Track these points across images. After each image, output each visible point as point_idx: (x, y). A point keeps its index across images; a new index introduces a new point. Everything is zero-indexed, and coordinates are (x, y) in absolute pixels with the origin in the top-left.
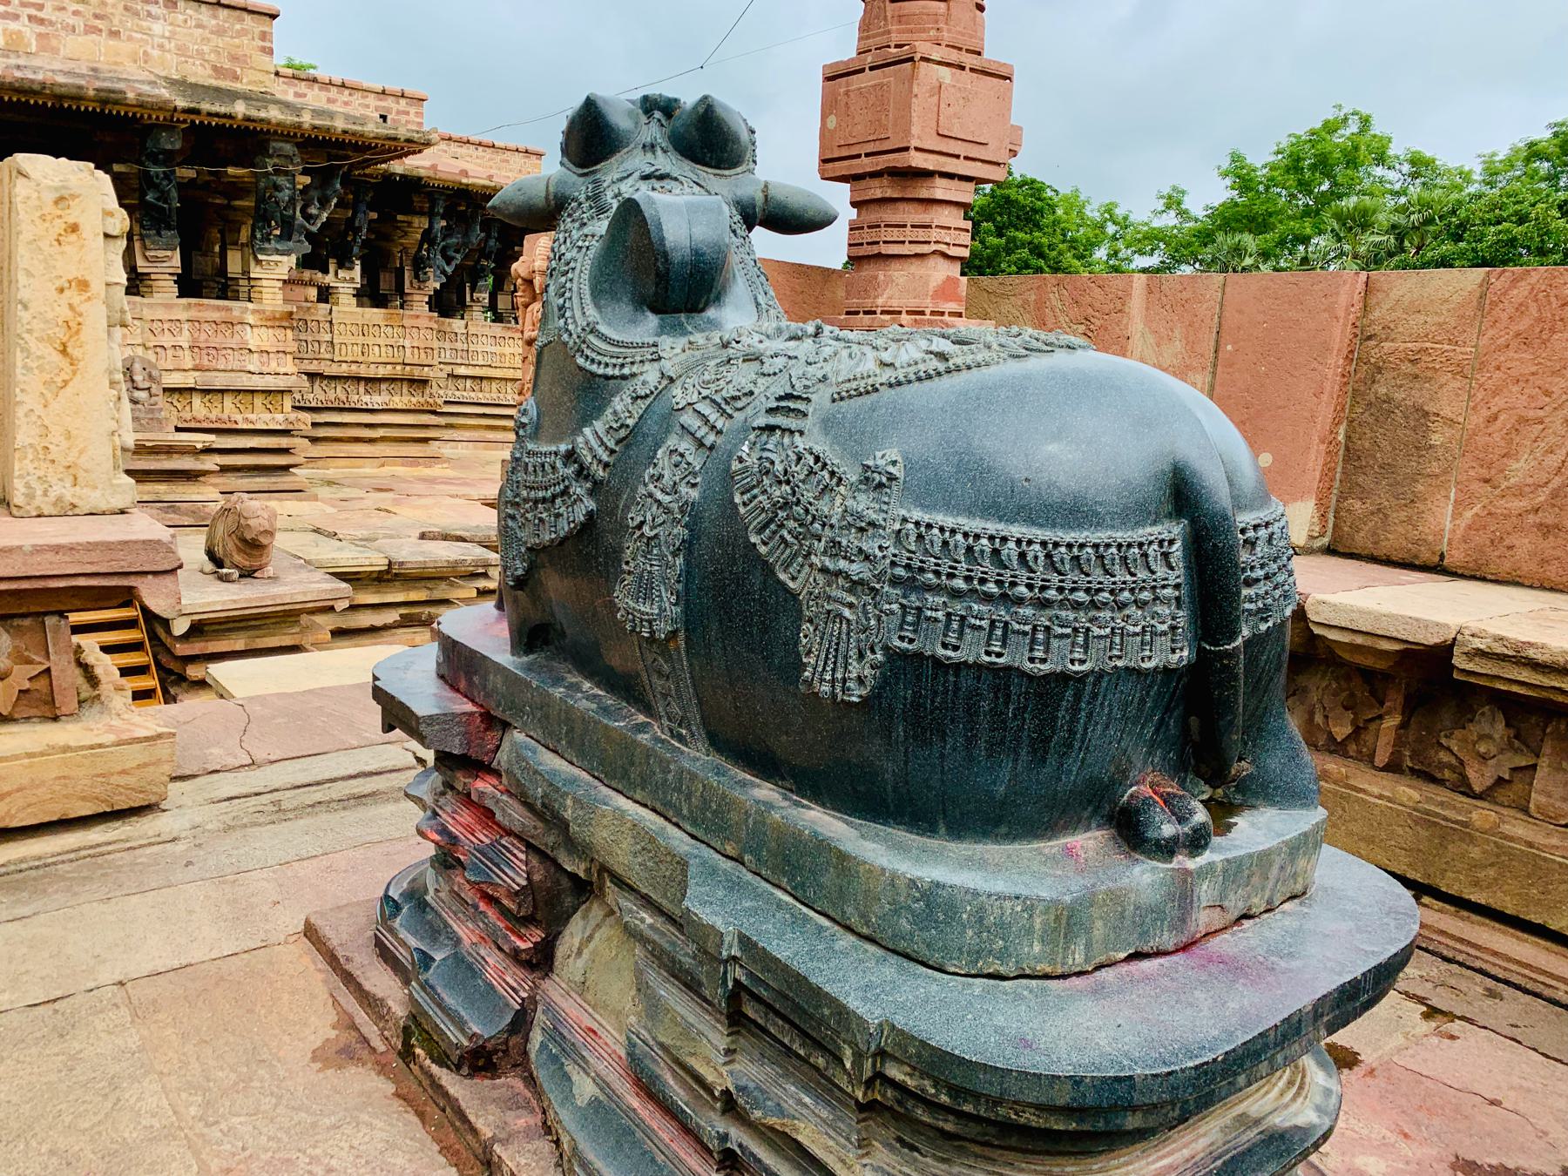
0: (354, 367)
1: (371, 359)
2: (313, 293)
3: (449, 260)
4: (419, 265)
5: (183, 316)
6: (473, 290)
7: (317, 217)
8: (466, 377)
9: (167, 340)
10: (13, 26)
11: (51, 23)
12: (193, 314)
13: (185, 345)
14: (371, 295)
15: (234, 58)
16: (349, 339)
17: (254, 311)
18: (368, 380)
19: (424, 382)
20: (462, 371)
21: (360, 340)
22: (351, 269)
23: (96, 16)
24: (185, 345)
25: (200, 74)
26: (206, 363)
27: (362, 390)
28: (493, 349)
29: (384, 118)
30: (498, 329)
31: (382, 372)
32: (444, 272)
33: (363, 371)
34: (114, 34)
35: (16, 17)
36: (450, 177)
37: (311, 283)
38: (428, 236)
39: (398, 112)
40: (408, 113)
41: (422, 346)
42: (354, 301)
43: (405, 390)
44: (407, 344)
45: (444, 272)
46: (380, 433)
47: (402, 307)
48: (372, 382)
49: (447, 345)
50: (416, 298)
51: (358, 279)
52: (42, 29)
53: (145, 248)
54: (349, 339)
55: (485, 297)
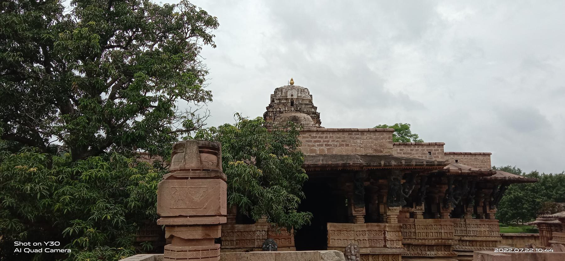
0: (423, 241)
1: (430, 238)
2: (408, 215)
3: (456, 199)
4: (445, 202)
5: (366, 229)
6: (467, 208)
7: (408, 192)
8: (466, 241)
9: (361, 238)
10: (321, 148)
11: (331, 145)
12: (370, 228)
13: (367, 239)
14: (428, 214)
15: (381, 146)
16: (422, 231)
17: (388, 226)
18: (429, 246)
19: (450, 246)
20: (466, 238)
21: (425, 231)
22: (421, 205)
23: (342, 141)
24: (367, 239)
25: (370, 152)
26: (373, 245)
27: (427, 249)
28: (477, 229)
29: (430, 153)
30: (478, 221)
31: (433, 242)
32: (455, 204)
33: (427, 242)
34: (347, 145)
35: (322, 145)
36: (455, 171)
37: (408, 212)
38: (448, 191)
39: (435, 150)
40: (438, 150)
41: (448, 232)
42: (422, 217)
43: (443, 249)
44: (443, 231)
45: (455, 204)
47: (440, 218)
48: (431, 247)
49: (458, 229)
50: (445, 214)
51: (424, 209)
52: (329, 147)
53: (355, 208)
54: (422, 231)
55: (471, 209)
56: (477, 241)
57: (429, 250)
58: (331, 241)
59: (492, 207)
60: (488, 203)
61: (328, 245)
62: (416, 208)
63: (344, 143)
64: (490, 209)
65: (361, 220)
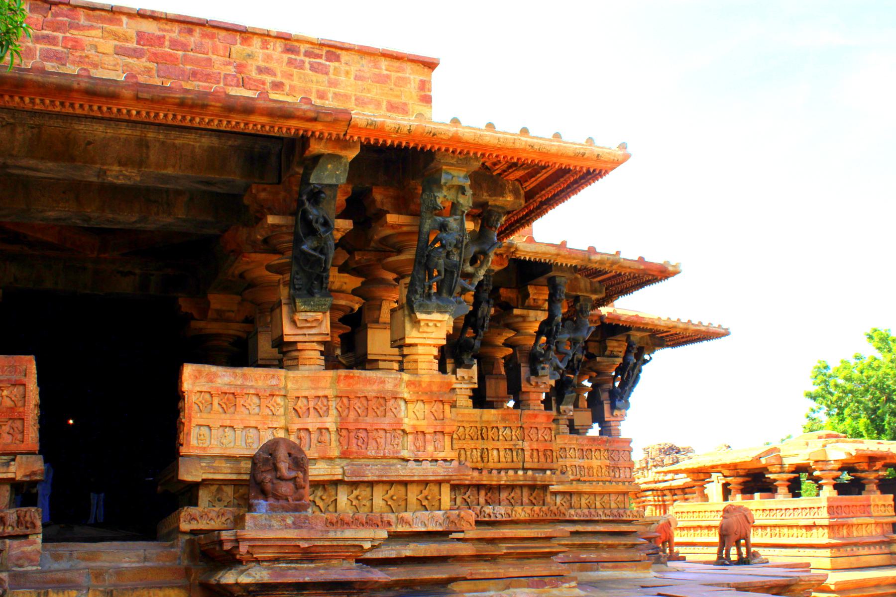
1: (491, 465)
6: (559, 403)
9: (312, 422)
17: (410, 384)
18: (489, 488)
21: (480, 444)
22: (469, 367)
24: (332, 427)
42: (470, 403)
44: (526, 445)
46: (503, 549)
56: (580, 494)
57: (487, 503)
58: (194, 432)
59: (618, 404)
60: (605, 396)
61: (183, 450)
62: (454, 372)
63: (268, 79)
64: (613, 407)
65: (313, 355)
